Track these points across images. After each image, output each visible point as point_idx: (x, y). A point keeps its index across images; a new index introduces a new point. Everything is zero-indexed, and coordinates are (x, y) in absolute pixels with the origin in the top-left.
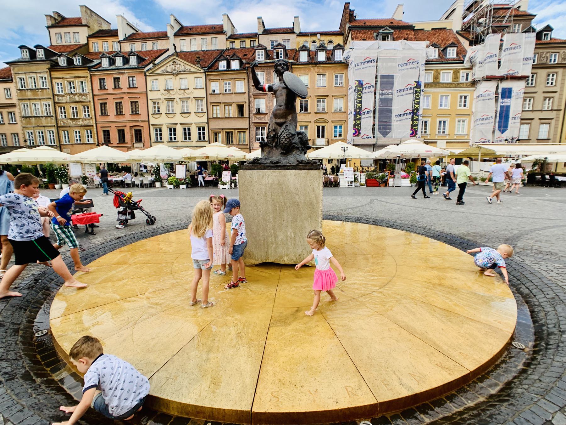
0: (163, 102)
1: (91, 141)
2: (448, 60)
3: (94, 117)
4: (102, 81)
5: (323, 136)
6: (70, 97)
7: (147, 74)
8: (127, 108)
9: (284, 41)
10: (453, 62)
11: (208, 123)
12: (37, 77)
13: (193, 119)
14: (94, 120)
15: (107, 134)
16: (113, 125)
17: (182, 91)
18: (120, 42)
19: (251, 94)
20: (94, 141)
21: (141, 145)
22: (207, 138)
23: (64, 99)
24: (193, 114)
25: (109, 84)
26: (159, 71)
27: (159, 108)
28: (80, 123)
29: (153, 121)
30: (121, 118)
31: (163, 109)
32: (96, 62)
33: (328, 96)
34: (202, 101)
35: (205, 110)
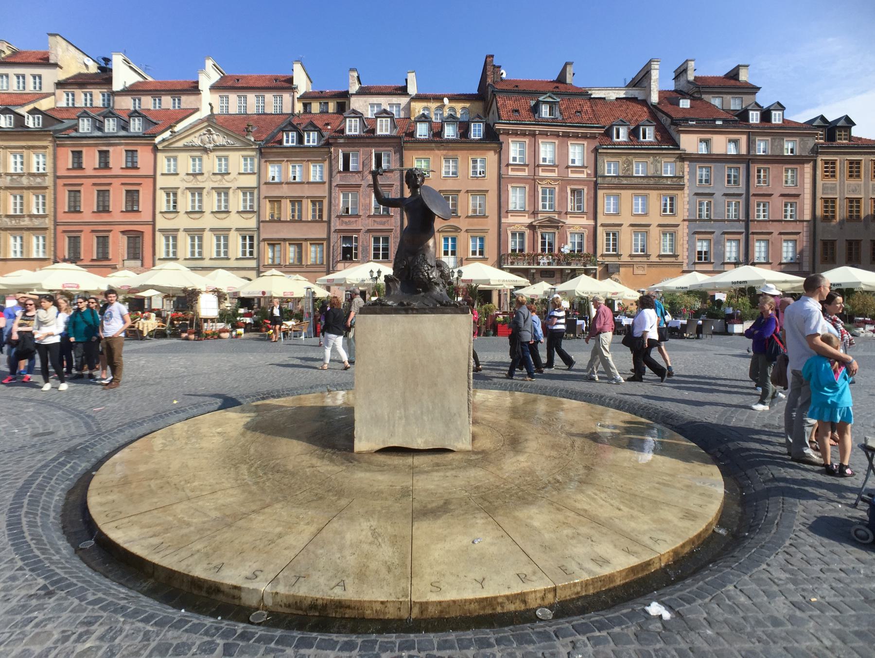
0: (183, 193)
3: (52, 214)
4: (77, 155)
5: (453, 253)
6: (12, 180)
7: (160, 147)
8: (118, 200)
9: (391, 105)
10: (649, 147)
11: (258, 228)
13: (234, 221)
14: (52, 218)
17: (219, 177)
19: (334, 184)
21: (139, 263)
22: (255, 255)
25: (90, 159)
27: (175, 202)
28: (26, 222)
29: (162, 223)
30: (105, 218)
31: (185, 202)
32: (67, 123)
33: (459, 191)
34: (252, 194)
35: (255, 209)
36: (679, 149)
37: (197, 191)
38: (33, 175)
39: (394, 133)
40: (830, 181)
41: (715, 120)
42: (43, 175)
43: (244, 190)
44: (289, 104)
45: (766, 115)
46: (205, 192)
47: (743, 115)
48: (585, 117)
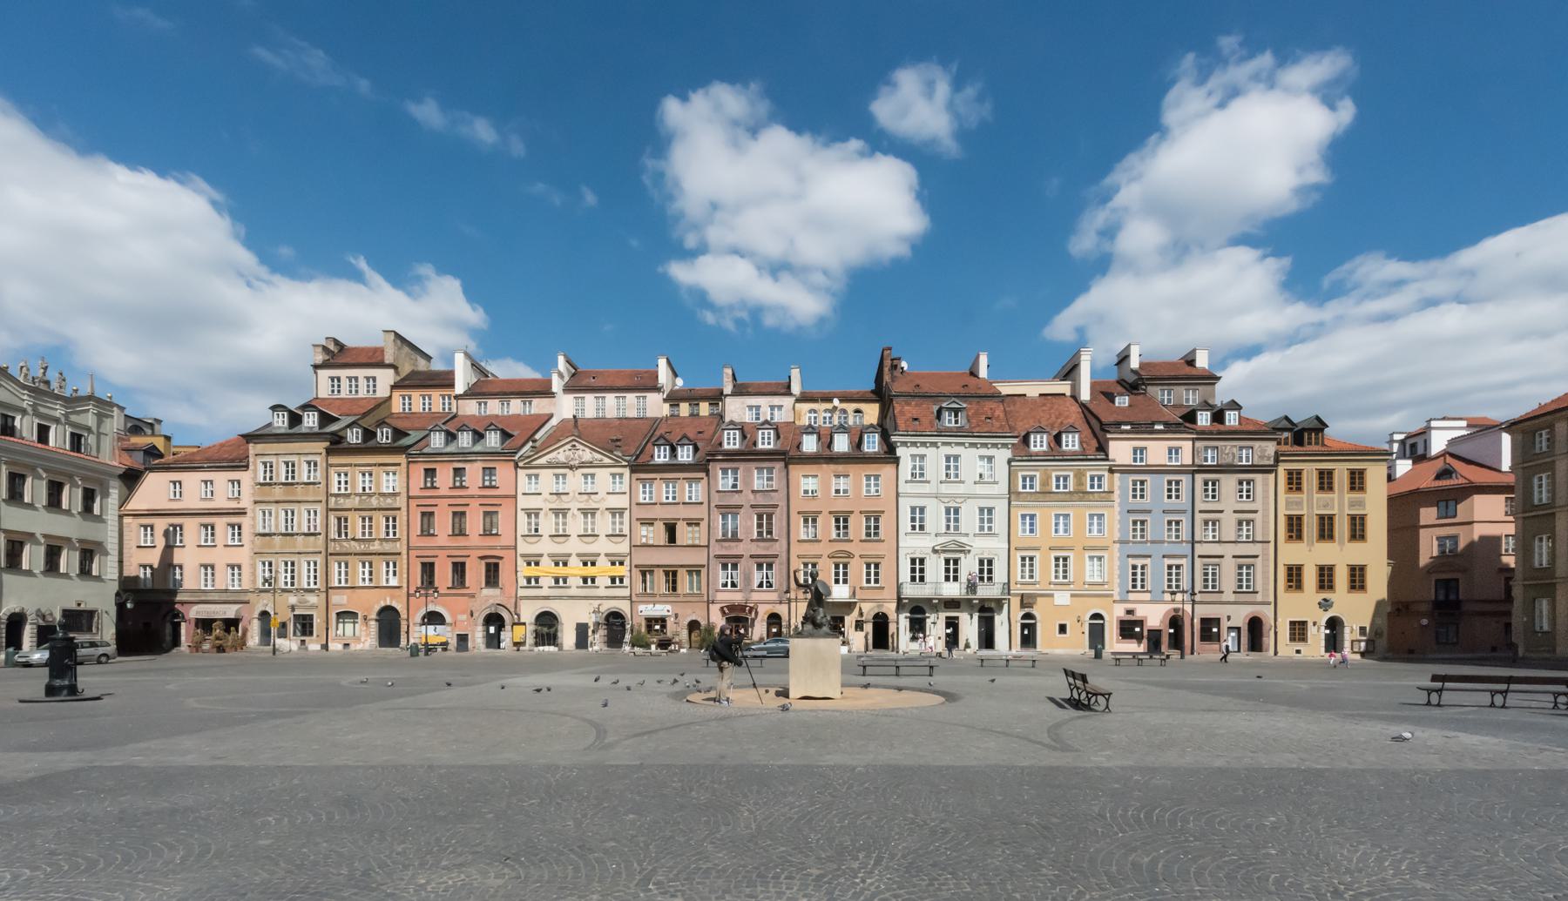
1: (393, 582)
2: (1064, 453)
5: (845, 581)
8: (474, 523)
12: (307, 461)
13: (603, 546)
15: (428, 569)
16: (442, 554)
18: (457, 397)
20: (400, 580)
23: (348, 503)
24: (602, 538)
26: (543, 461)
28: (376, 547)
29: (524, 547)
30: (461, 542)
31: (547, 524)
34: (621, 514)
35: (626, 531)
36: (1107, 459)
37: (560, 512)
38: (383, 495)
39: (778, 447)
40: (1295, 496)
41: (1153, 424)
42: (394, 495)
43: (616, 512)
44: (656, 406)
45: (1218, 417)
46: (569, 515)
47: (1190, 417)
48: (997, 424)
